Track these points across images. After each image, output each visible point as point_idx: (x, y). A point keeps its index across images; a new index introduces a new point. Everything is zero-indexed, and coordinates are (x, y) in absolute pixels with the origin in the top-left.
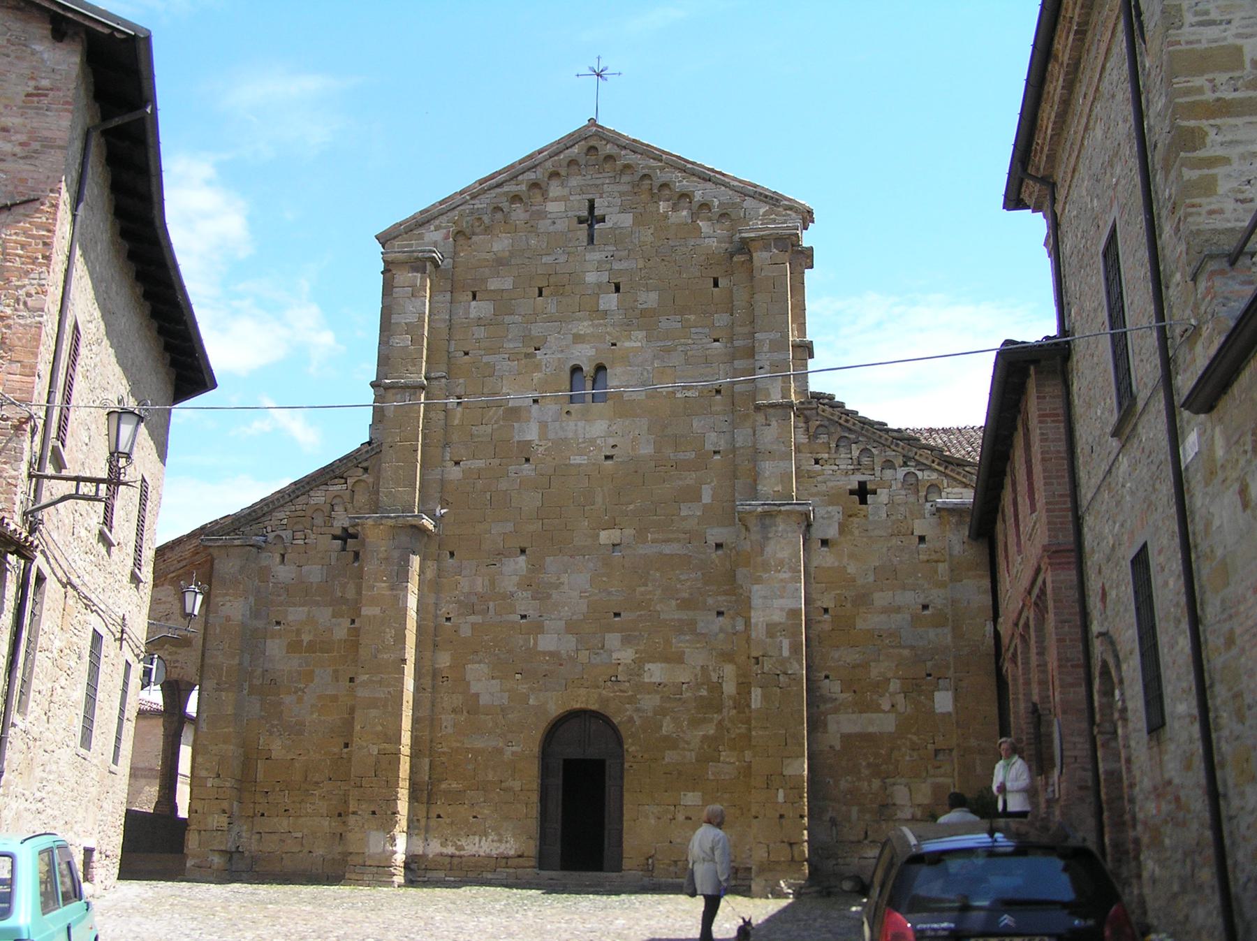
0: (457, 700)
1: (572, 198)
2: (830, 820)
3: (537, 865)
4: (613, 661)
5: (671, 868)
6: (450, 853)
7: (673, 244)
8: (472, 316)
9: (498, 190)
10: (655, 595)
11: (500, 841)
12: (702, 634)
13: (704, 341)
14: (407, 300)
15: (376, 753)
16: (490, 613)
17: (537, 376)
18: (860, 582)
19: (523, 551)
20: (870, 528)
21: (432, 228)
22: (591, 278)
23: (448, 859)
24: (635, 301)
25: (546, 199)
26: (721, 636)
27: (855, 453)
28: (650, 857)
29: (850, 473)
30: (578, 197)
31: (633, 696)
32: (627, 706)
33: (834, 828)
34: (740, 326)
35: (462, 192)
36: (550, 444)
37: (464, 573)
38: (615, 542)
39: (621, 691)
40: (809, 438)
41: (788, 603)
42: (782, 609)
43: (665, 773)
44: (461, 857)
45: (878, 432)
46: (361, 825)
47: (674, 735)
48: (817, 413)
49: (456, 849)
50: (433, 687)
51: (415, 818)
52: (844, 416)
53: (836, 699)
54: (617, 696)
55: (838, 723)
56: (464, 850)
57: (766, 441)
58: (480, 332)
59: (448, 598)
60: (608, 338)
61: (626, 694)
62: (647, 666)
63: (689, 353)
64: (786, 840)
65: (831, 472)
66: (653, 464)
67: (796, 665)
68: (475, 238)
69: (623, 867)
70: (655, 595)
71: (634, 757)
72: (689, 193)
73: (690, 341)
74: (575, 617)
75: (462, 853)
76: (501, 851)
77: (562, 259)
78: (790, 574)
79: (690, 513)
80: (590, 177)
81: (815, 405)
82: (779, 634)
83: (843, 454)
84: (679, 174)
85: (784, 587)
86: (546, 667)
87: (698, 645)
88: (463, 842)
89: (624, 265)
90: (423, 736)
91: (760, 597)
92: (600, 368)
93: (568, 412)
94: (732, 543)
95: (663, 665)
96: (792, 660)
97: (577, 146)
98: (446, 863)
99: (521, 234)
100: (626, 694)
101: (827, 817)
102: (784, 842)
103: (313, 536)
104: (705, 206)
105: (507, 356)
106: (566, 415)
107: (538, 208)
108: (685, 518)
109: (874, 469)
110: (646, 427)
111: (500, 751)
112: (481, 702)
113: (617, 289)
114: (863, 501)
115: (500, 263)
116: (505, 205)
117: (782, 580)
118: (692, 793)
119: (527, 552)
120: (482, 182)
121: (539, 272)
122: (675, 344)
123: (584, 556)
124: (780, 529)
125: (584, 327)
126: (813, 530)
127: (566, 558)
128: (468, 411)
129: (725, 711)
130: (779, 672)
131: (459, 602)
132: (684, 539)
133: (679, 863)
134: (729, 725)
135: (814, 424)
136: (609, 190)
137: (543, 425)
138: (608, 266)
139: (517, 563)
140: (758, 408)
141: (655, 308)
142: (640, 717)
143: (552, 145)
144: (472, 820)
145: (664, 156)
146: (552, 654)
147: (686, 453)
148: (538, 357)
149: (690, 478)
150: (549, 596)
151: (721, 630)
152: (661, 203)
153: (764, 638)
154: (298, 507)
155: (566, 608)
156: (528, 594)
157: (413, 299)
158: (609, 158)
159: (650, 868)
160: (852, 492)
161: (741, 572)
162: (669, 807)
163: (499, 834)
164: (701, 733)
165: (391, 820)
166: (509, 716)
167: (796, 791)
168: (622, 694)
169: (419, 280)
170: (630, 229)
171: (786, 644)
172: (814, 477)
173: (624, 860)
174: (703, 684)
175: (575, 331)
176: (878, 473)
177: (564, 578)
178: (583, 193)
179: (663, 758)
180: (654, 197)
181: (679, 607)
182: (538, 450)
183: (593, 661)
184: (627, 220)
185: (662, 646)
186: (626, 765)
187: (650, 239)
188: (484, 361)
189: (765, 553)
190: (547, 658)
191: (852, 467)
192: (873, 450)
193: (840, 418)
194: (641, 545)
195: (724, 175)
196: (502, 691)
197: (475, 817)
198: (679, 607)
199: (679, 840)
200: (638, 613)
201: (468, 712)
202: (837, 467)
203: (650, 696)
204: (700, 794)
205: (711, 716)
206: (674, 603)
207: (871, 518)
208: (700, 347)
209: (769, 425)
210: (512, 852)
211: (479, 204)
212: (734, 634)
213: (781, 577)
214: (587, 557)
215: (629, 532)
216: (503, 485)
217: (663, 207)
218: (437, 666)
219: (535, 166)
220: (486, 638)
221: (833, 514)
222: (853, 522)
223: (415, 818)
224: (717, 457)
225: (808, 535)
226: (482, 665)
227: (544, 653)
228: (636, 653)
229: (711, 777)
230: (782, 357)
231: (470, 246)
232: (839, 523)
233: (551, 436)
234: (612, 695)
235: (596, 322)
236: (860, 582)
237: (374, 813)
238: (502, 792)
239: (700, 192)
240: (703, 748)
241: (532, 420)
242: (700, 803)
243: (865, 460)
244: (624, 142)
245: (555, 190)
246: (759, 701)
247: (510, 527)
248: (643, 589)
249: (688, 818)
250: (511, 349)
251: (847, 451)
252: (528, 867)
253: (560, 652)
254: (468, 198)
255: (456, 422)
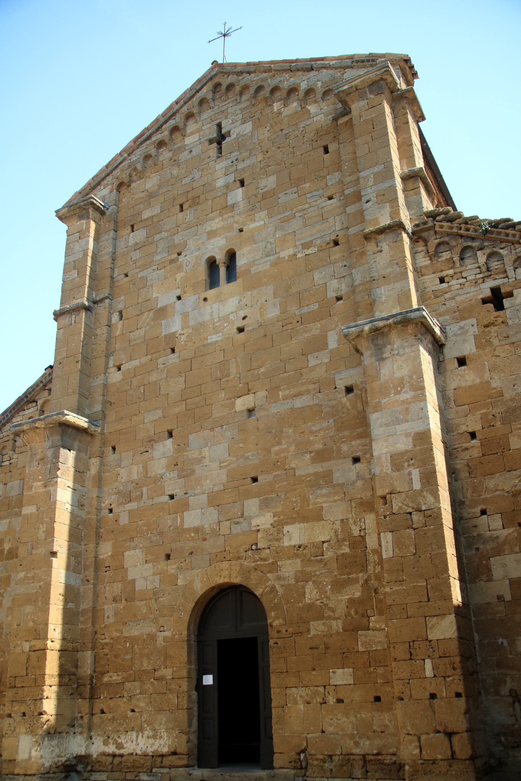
0: (117, 588)
1: (203, 128)
2: (510, 695)
3: (196, 763)
4: (253, 529)
5: (327, 765)
6: (111, 752)
7: (287, 132)
8: (130, 244)
9: (148, 142)
10: (289, 452)
11: (154, 737)
12: (339, 485)
13: (319, 202)
14: (76, 243)
15: (27, 650)
16: (143, 498)
17: (179, 276)
18: (507, 395)
19: (170, 434)
20: (511, 333)
21: (102, 187)
22: (220, 183)
23: (110, 759)
24: (257, 189)
25: (184, 136)
26: (360, 483)
27: (482, 257)
28: (303, 751)
29: (479, 282)
30: (209, 125)
31: (274, 563)
32: (268, 575)
33: (517, 704)
34: (349, 176)
35: (121, 154)
36: (191, 331)
37: (123, 464)
38: (251, 406)
39: (262, 559)
40: (431, 259)
41: (415, 427)
42: (407, 435)
43: (311, 648)
44: (122, 756)
45: (503, 231)
46: (13, 729)
47: (318, 602)
48: (436, 233)
49: (117, 748)
50: (96, 578)
51: (80, 715)
52: (463, 226)
53: (497, 537)
54: (258, 565)
55: (504, 565)
56: (123, 748)
57: (379, 267)
58: (136, 255)
59: (110, 490)
60: (235, 226)
61: (267, 563)
62: (286, 528)
63: (306, 216)
64: (442, 730)
65: (459, 286)
66: (280, 324)
67: (430, 499)
68: (133, 185)
69: (275, 765)
70: (289, 452)
71: (279, 632)
72: (296, 86)
73: (307, 206)
74: (216, 489)
75: (122, 751)
76: (155, 748)
77: (197, 175)
78: (413, 393)
79: (318, 362)
80: (217, 107)
81: (430, 224)
82: (406, 464)
83: (469, 264)
84: (287, 75)
85: (407, 409)
86: (192, 544)
87: (336, 498)
88: (122, 740)
89: (247, 163)
90: (86, 628)
91: (381, 426)
92: (231, 256)
93: (205, 299)
94: (362, 382)
95: (302, 525)
96: (425, 493)
97: (205, 87)
98: (107, 764)
99: (166, 169)
100: (267, 563)
101: (505, 690)
102: (438, 732)
103: (15, 456)
104: (309, 91)
105: (155, 267)
106: (203, 302)
107: (179, 145)
108: (313, 368)
109: (505, 272)
110: (272, 292)
111: (153, 638)
112: (137, 589)
113: (242, 183)
114: (500, 307)
115: (151, 195)
116: (153, 151)
117: (403, 402)
118: (340, 671)
119: (173, 435)
120: (135, 140)
121: (180, 192)
122: (293, 212)
123: (222, 426)
124: (395, 346)
125: (216, 224)
126: (446, 350)
127: (207, 432)
128: (126, 321)
129: (370, 568)
130: (411, 510)
131: (119, 493)
132: (315, 389)
133: (334, 758)
134: (376, 584)
135: (433, 242)
136: (233, 110)
137: (185, 316)
138: (234, 168)
139: (165, 446)
140: (367, 237)
141: (274, 189)
142: (282, 586)
143: (185, 93)
144: (130, 714)
145: (272, 66)
146: (197, 530)
147: (310, 306)
148: (180, 260)
149: (315, 329)
150: (193, 472)
151: (359, 477)
152: (275, 104)
153: (389, 472)
154: (5, 434)
155: (208, 481)
156: (175, 474)
157: (80, 241)
158: (230, 87)
159: (304, 764)
160: (485, 301)
161: (369, 410)
162: (319, 688)
163: (154, 730)
164: (347, 597)
165: (37, 721)
166: (161, 599)
167: (447, 660)
168: (262, 563)
169: (85, 225)
170: (250, 133)
171: (416, 474)
172: (442, 295)
173: (275, 756)
174: (344, 540)
175: (209, 229)
176: (511, 273)
177: (206, 452)
178: (213, 121)
179: (309, 630)
180: (268, 102)
181: (314, 461)
182: (181, 338)
183: (234, 531)
184: (248, 127)
185: (299, 505)
186: (271, 642)
187: (267, 134)
188: (139, 276)
189: (382, 375)
190: (193, 535)
191: (481, 276)
192: (501, 251)
193: (461, 230)
194: (273, 405)
195: (322, 59)
196: (154, 574)
197: (133, 711)
198: (314, 461)
199: (331, 729)
200: (274, 474)
201: (126, 600)
202: (464, 280)
203: (290, 561)
204: (351, 670)
205: (354, 576)
206: (308, 456)
207: (510, 322)
208: (315, 208)
209: (381, 251)
210: (165, 750)
211: (133, 158)
212: (371, 479)
213: (402, 399)
214: (224, 427)
215: (262, 394)
216: (154, 377)
217: (276, 106)
218: (101, 557)
219: (174, 114)
220: (140, 523)
221: (466, 328)
222: (490, 332)
223: (80, 715)
224: (341, 302)
225: (441, 356)
226: (137, 550)
227: (189, 530)
228: (274, 516)
229: (361, 649)
230: (387, 185)
231: (130, 192)
232: (475, 336)
233: (192, 323)
234: (253, 564)
235: (225, 216)
236: (507, 395)
237: (24, 714)
238: (155, 682)
239: (305, 82)
240: (349, 614)
241: (176, 314)
242: (352, 682)
243: (494, 264)
244: (239, 69)
245: (191, 127)
246: (391, 549)
247: (159, 414)
248: (277, 448)
249: (340, 701)
250: (159, 260)
251: (472, 262)
252: (181, 767)
253: (203, 527)
254: (126, 155)
255: (118, 333)
